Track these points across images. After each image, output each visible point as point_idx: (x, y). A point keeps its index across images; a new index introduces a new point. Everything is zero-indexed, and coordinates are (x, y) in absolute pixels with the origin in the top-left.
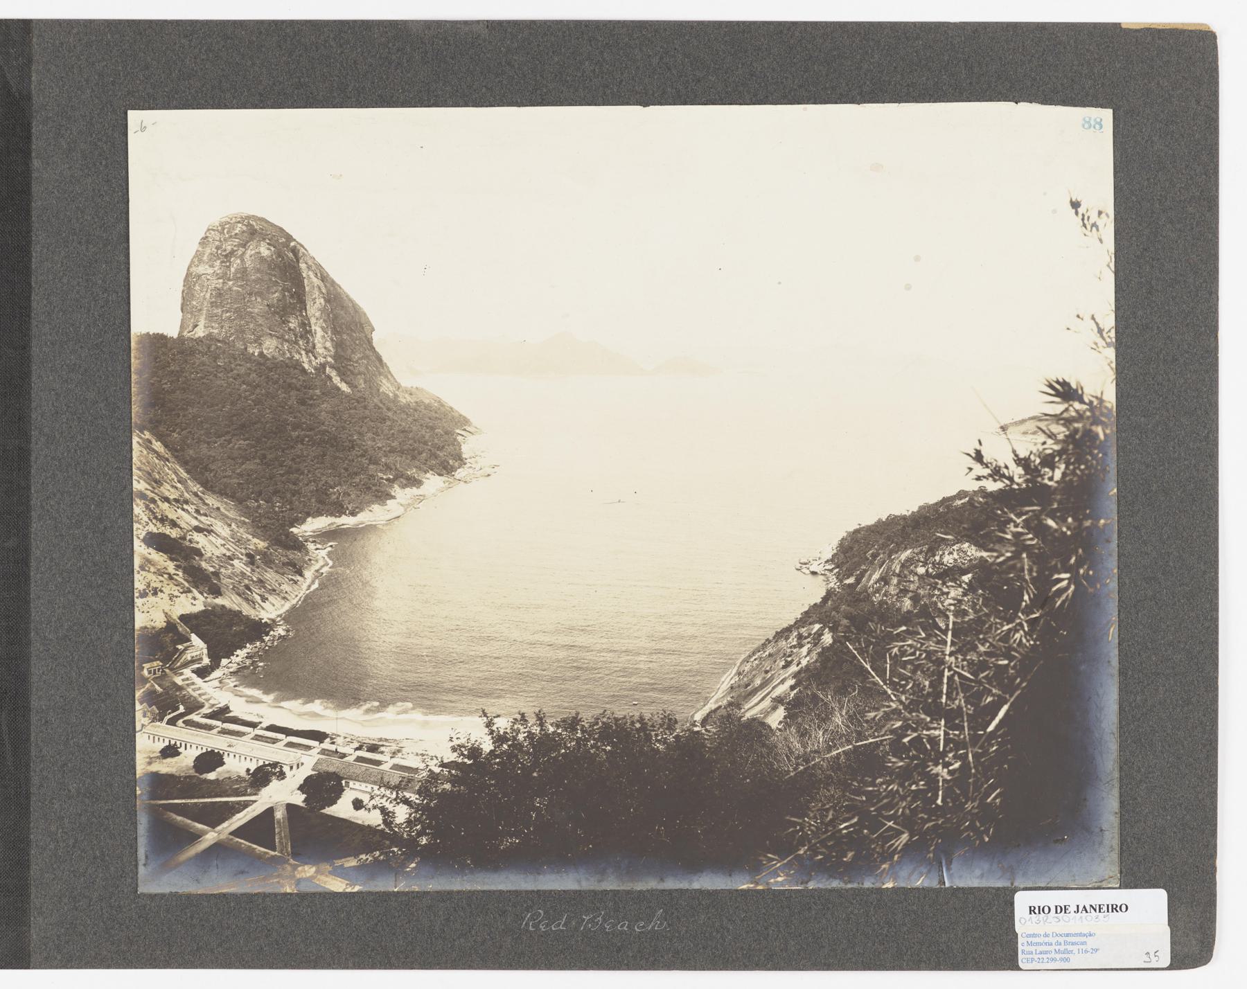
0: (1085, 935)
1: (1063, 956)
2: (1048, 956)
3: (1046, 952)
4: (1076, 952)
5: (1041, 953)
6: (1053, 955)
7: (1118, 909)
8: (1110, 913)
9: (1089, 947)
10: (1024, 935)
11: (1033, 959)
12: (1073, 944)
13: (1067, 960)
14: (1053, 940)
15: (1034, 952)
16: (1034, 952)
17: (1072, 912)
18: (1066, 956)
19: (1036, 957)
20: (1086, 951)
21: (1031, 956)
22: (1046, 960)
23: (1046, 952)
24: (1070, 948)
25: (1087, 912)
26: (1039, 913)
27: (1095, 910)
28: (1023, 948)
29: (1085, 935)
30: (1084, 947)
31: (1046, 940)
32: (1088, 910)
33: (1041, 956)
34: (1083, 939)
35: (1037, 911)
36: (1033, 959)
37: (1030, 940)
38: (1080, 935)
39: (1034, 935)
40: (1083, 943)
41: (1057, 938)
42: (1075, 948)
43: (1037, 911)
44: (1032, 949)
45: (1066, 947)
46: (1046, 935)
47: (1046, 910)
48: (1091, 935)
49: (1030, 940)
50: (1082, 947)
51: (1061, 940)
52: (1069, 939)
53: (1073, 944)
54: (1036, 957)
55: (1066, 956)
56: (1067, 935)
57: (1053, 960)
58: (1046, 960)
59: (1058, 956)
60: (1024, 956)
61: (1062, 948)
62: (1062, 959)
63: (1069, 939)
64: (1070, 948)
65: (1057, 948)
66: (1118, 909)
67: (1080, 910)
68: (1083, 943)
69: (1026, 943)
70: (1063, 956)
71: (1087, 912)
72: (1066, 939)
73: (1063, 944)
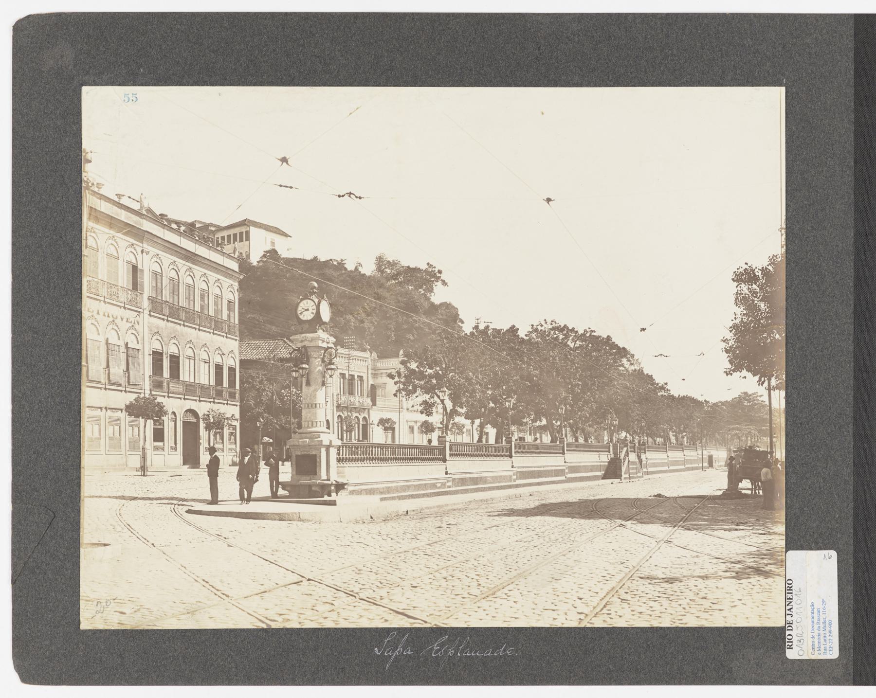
0: (813, 610)
1: (827, 625)
2: (828, 635)
3: (825, 637)
4: (824, 616)
5: (825, 641)
7: (790, 586)
8: (793, 592)
9: (821, 607)
10: (813, 653)
11: (830, 647)
12: (819, 618)
13: (830, 622)
14: (816, 632)
17: (792, 619)
18: (827, 623)
19: (828, 646)
20: (824, 608)
21: (828, 648)
22: (831, 638)
23: (825, 637)
24: (822, 621)
25: (792, 608)
26: (792, 642)
27: (791, 602)
28: (822, 654)
29: (813, 610)
30: (821, 610)
31: (816, 637)
32: (791, 607)
33: (828, 641)
34: (816, 610)
35: (790, 644)
36: (830, 647)
37: (816, 649)
38: (813, 613)
39: (813, 646)
40: (819, 610)
42: (822, 617)
43: (790, 644)
44: (822, 647)
45: (821, 623)
46: (813, 637)
47: (790, 637)
48: (813, 605)
49: (816, 649)
50: (821, 613)
51: (816, 627)
52: (816, 621)
53: (819, 618)
54: (828, 646)
55: (827, 623)
56: (813, 622)
57: (830, 632)
58: (831, 638)
59: (828, 629)
60: (828, 652)
61: (822, 626)
62: (830, 626)
63: (816, 621)
64: (822, 621)
65: (822, 629)
66: (790, 586)
67: (791, 613)
68: (819, 610)
69: (819, 652)
70: (827, 625)
71: (792, 608)
72: (815, 623)
73: (819, 625)
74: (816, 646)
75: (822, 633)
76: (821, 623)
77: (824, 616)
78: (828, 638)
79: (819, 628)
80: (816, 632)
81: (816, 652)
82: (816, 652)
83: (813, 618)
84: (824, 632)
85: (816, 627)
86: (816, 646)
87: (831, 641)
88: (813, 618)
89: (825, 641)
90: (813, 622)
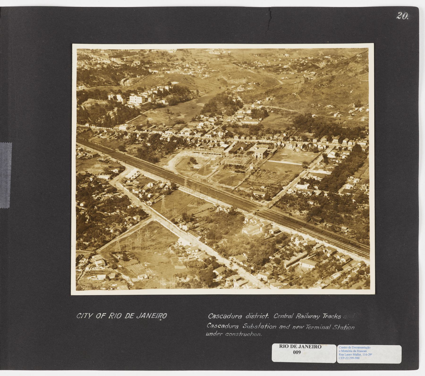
0: (366, 348)
3: (349, 355)
5: (347, 355)
6: (352, 356)
9: (367, 353)
10: (340, 347)
11: (344, 358)
12: (362, 351)
13: (358, 358)
14: (353, 350)
15: (344, 355)
16: (344, 355)
19: (344, 356)
20: (367, 355)
22: (349, 358)
23: (349, 355)
24: (359, 353)
28: (340, 353)
29: (366, 348)
30: (365, 353)
31: (350, 349)
33: (347, 356)
36: (344, 358)
37: (343, 349)
40: (365, 351)
41: (354, 349)
42: (362, 353)
44: (343, 353)
45: (358, 353)
49: (343, 349)
50: (364, 353)
51: (356, 349)
54: (344, 356)
55: (358, 356)
56: (359, 348)
58: (349, 358)
59: (354, 356)
61: (356, 353)
62: (356, 358)
64: (359, 353)
68: (365, 351)
73: (357, 351)
74: (345, 349)
75: (352, 353)
76: (358, 353)
77: (362, 354)
78: (349, 356)
79: (355, 351)
80: (353, 350)
81: (341, 349)
82: (341, 349)
83: (361, 348)
84: (352, 354)
85: (356, 349)
86: (345, 349)
87: (347, 358)
88: (361, 348)
89: (347, 355)
90: (359, 348)
